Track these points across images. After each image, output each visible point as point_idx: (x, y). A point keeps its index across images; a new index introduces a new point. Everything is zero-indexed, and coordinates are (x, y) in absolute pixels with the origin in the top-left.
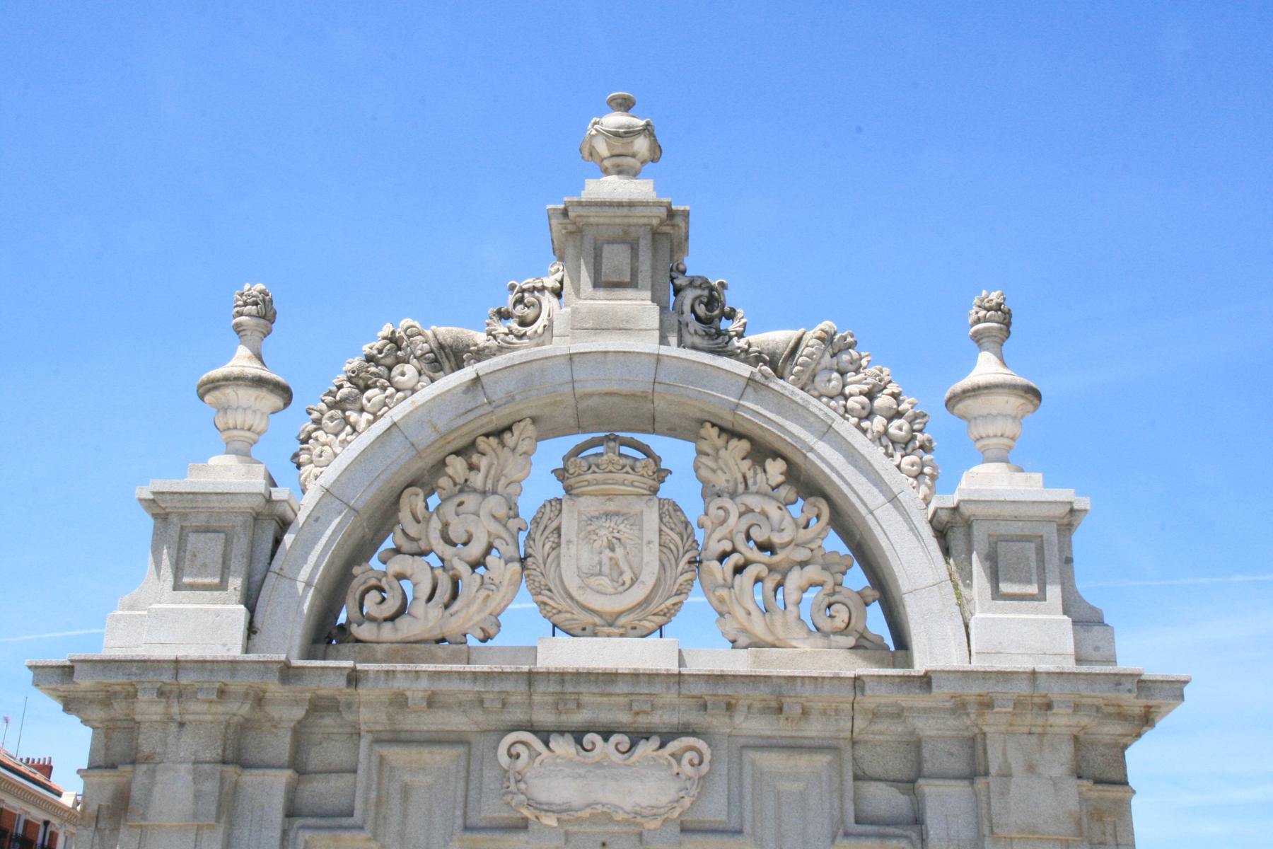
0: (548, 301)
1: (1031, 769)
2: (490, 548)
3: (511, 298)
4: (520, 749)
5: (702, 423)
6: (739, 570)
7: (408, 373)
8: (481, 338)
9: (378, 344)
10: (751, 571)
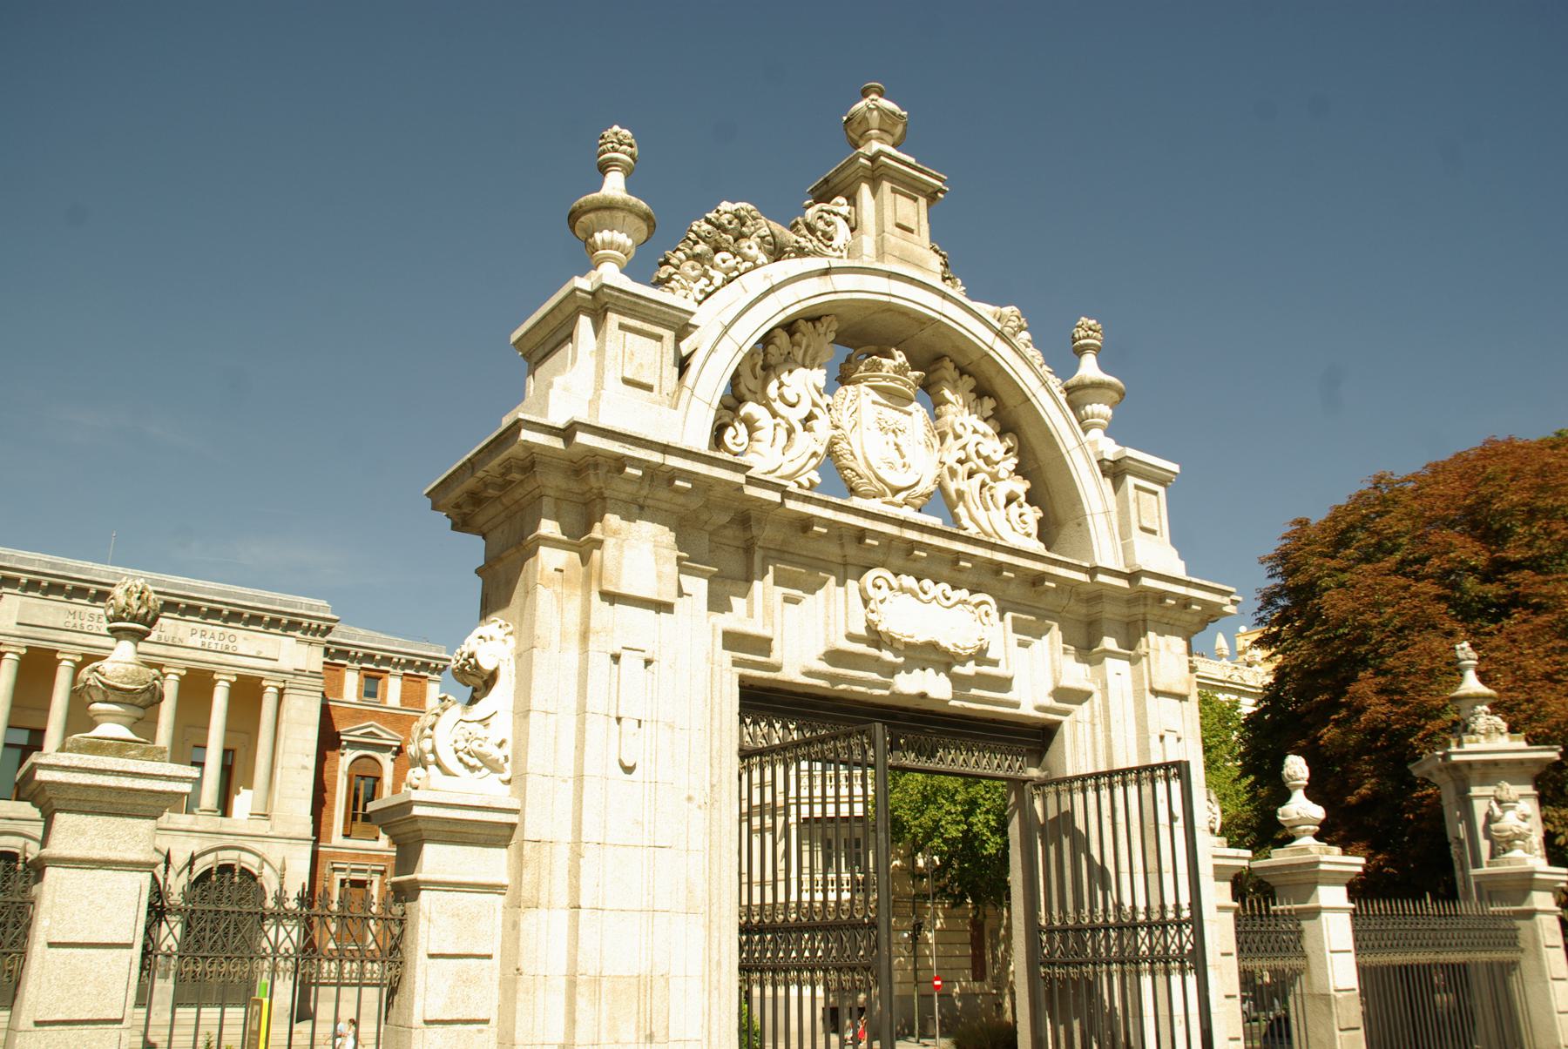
6: (970, 475)
10: (978, 478)
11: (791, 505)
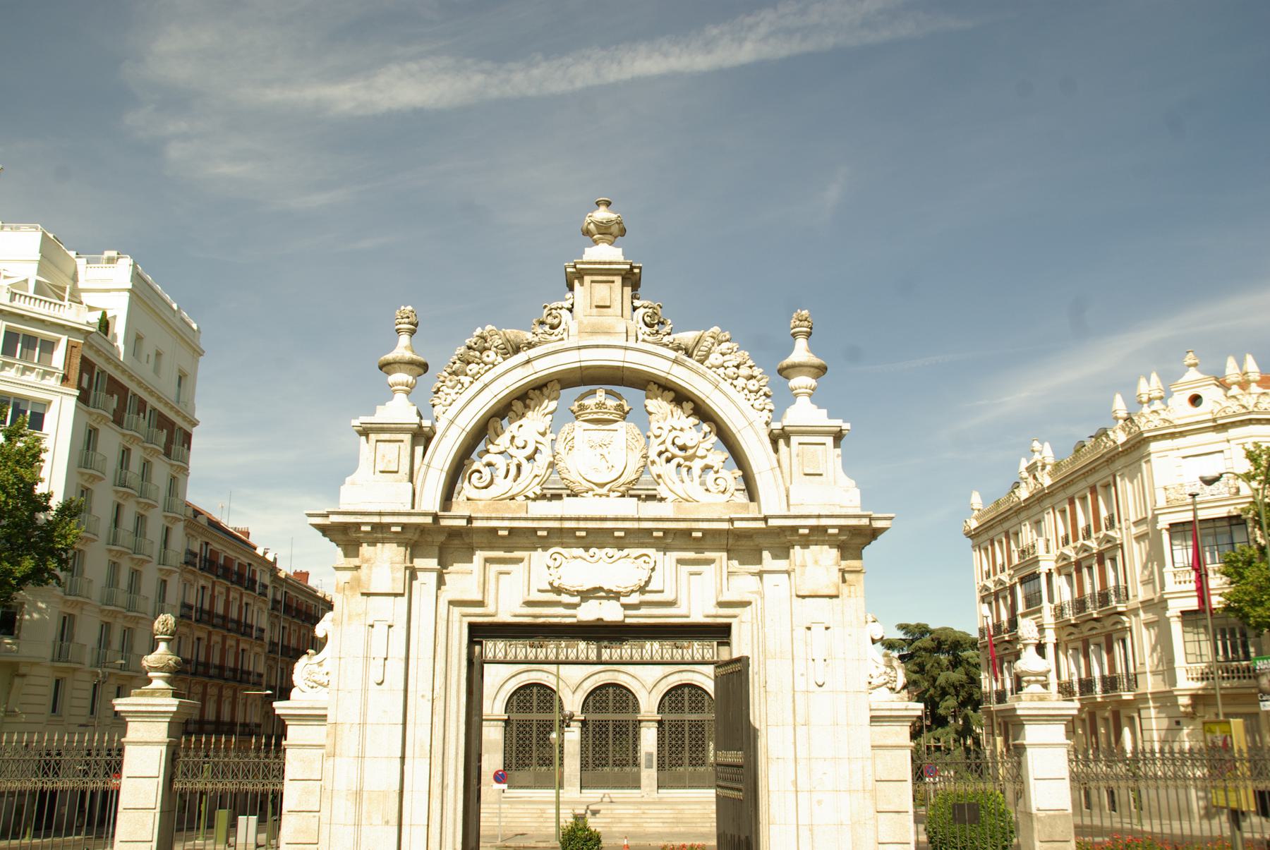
0: (565, 313)
1: (816, 562)
2: (536, 450)
3: (546, 312)
4: (556, 556)
5: (649, 382)
6: (668, 461)
7: (491, 356)
8: (529, 336)
9: (474, 340)
10: (674, 462)
11: (476, 524)
